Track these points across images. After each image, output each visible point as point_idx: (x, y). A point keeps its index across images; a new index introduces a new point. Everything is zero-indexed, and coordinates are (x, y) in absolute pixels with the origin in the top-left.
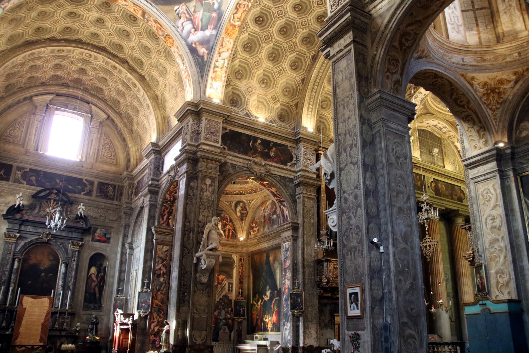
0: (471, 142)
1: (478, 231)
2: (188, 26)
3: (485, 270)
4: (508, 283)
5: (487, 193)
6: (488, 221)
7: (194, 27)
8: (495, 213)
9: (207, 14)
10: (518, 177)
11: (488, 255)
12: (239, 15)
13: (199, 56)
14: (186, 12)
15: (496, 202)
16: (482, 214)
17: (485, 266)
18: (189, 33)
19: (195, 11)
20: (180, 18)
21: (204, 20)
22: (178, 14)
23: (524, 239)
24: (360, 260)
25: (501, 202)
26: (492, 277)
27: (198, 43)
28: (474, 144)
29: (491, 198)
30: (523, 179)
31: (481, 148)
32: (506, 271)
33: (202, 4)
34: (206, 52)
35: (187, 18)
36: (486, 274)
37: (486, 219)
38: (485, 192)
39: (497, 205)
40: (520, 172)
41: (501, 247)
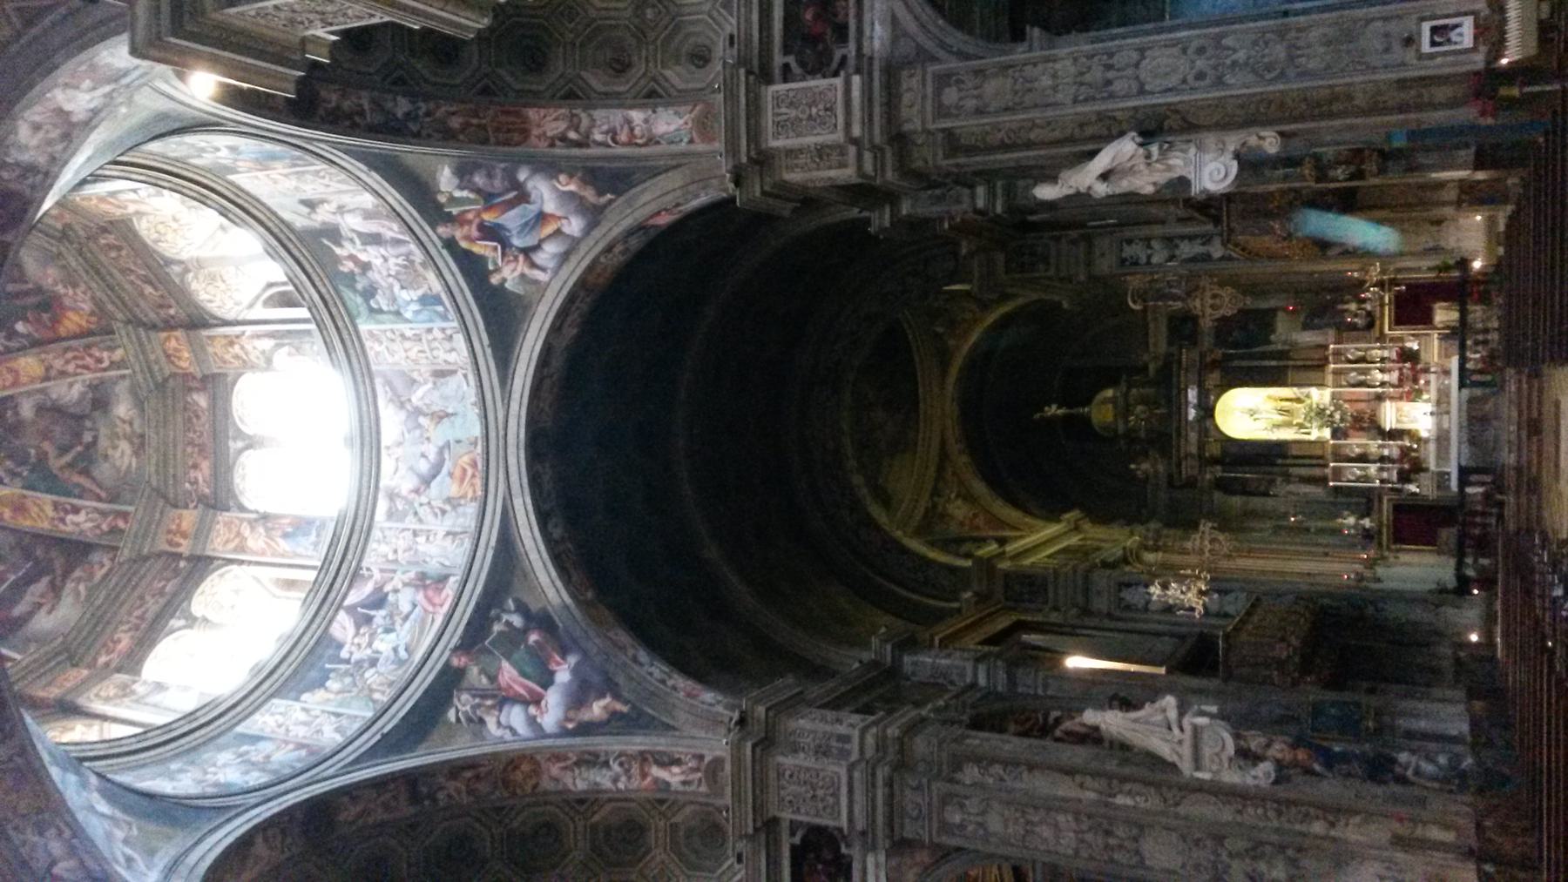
2: (516, 716)
7: (526, 703)
9: (520, 654)
12: (574, 579)
13: (609, 721)
14: (477, 700)
18: (532, 721)
19: (493, 679)
20: (482, 721)
21: (528, 670)
22: (470, 720)
24: (1314, 34)
27: (571, 714)
33: (490, 652)
34: (608, 700)
35: (493, 707)
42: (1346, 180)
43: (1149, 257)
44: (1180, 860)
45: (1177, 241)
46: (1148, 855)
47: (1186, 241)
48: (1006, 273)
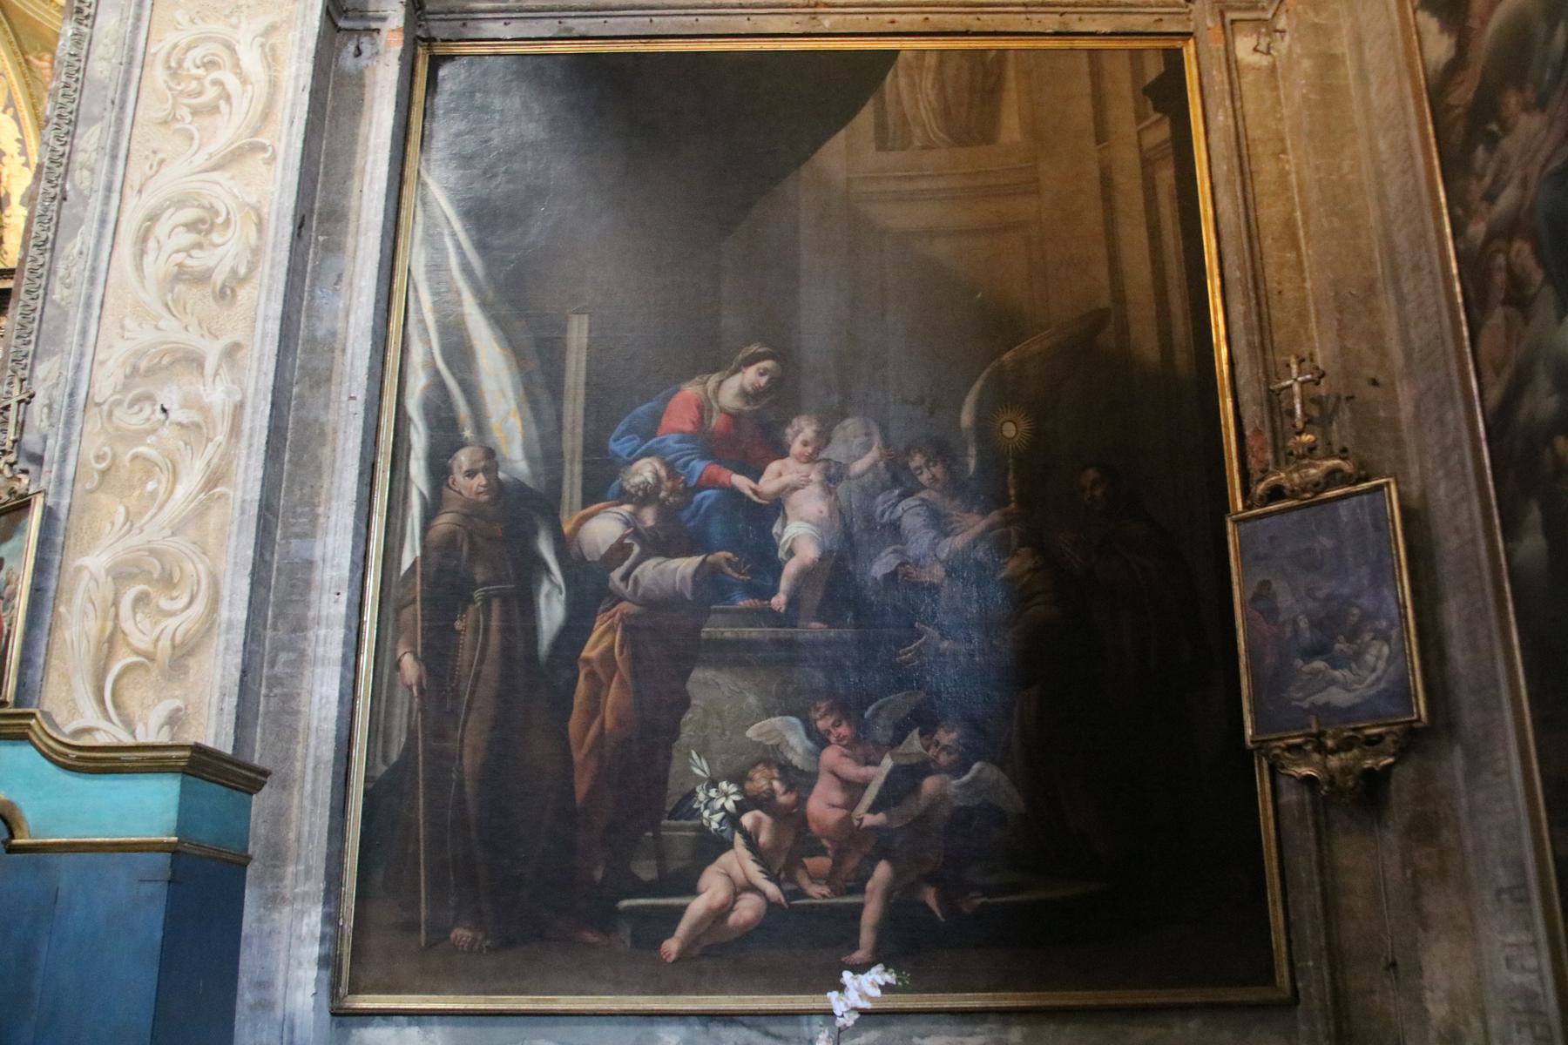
1: (58, 293)
3: (45, 542)
4: (183, 653)
5: (211, 64)
6: (161, 229)
8: (225, 191)
10: (420, 50)
11: (92, 442)
15: (256, 132)
16: (135, 177)
17: (49, 515)
23: (361, 395)
25: (288, 137)
26: (79, 599)
30: (443, 72)
32: (196, 569)
36: (41, 568)
37: (153, 218)
38: (197, 54)
40: (439, 30)
41: (204, 409)
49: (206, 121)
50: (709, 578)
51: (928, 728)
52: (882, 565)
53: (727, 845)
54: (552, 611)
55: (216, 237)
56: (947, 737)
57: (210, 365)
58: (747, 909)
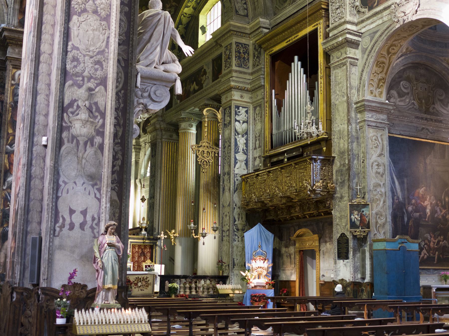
0: (370, 86)
4: (384, 224)
6: (374, 165)
8: (380, 160)
28: (372, 89)
29: (378, 145)
31: (375, 96)
32: (384, 214)
37: (373, 163)
38: (374, 138)
39: (382, 154)
41: (382, 192)
42: (351, 220)
43: (239, 121)
44: (81, 47)
45: (245, 137)
46: (81, 19)
47: (245, 141)
48: (236, 43)
49: (376, 149)
50: (420, 215)
51: (440, 237)
52: (436, 216)
53: (423, 249)
54: (406, 219)
55: (380, 167)
56: (442, 237)
57: (382, 186)
58: (426, 257)
